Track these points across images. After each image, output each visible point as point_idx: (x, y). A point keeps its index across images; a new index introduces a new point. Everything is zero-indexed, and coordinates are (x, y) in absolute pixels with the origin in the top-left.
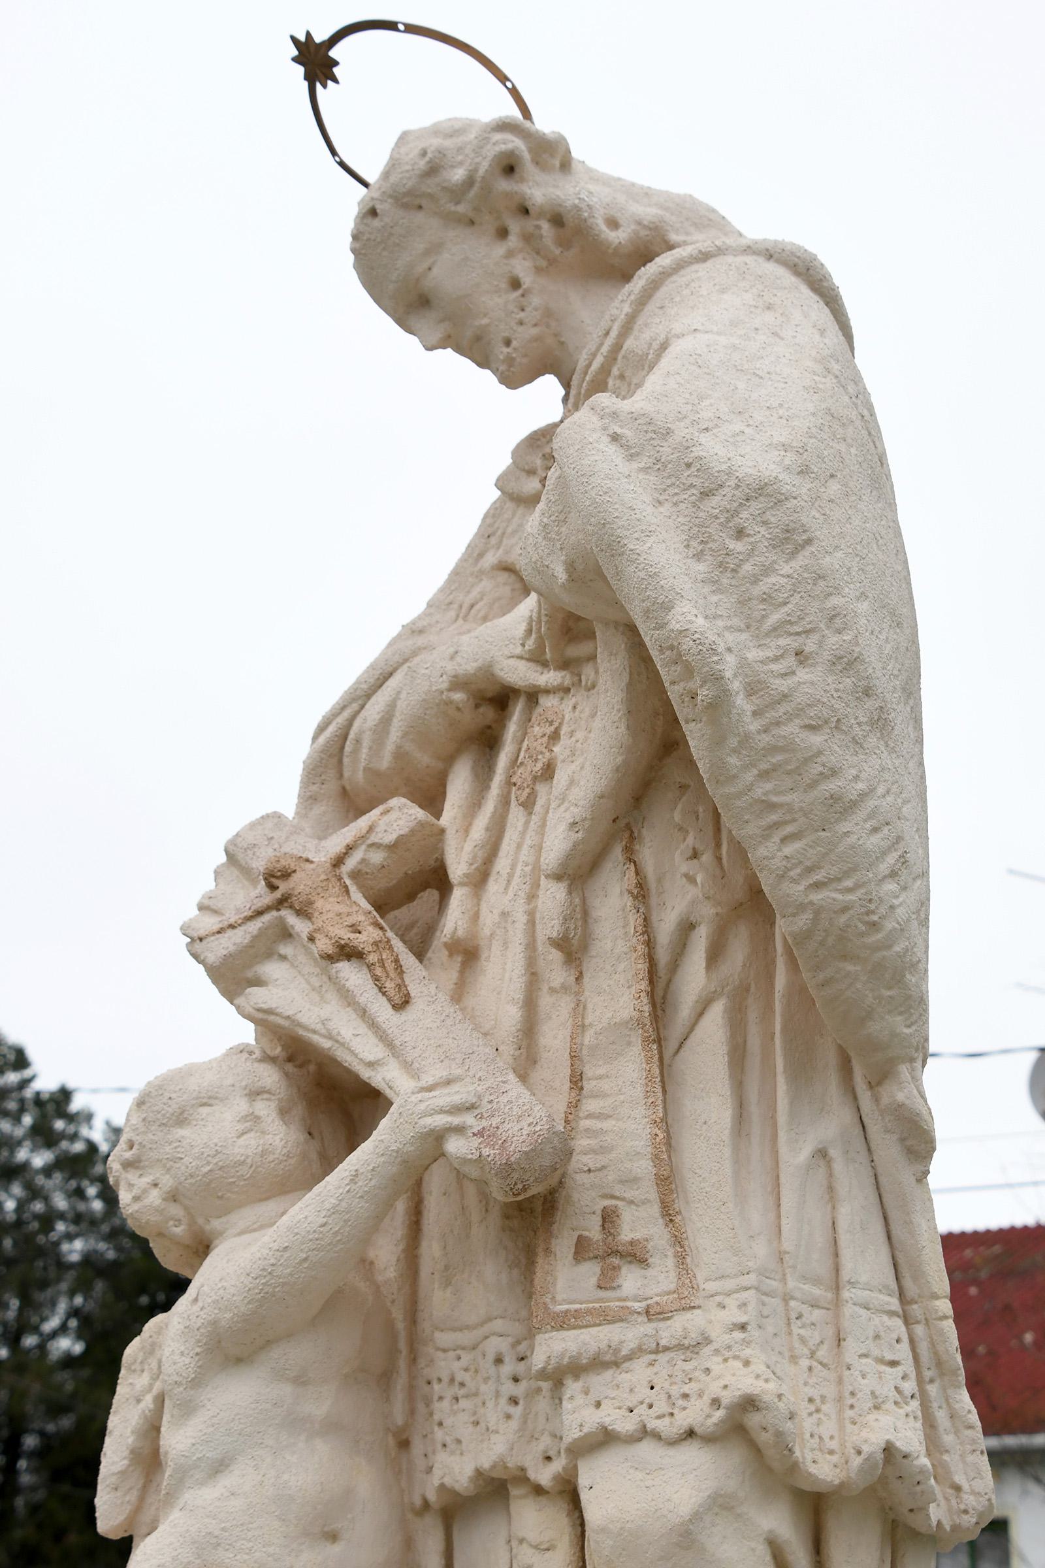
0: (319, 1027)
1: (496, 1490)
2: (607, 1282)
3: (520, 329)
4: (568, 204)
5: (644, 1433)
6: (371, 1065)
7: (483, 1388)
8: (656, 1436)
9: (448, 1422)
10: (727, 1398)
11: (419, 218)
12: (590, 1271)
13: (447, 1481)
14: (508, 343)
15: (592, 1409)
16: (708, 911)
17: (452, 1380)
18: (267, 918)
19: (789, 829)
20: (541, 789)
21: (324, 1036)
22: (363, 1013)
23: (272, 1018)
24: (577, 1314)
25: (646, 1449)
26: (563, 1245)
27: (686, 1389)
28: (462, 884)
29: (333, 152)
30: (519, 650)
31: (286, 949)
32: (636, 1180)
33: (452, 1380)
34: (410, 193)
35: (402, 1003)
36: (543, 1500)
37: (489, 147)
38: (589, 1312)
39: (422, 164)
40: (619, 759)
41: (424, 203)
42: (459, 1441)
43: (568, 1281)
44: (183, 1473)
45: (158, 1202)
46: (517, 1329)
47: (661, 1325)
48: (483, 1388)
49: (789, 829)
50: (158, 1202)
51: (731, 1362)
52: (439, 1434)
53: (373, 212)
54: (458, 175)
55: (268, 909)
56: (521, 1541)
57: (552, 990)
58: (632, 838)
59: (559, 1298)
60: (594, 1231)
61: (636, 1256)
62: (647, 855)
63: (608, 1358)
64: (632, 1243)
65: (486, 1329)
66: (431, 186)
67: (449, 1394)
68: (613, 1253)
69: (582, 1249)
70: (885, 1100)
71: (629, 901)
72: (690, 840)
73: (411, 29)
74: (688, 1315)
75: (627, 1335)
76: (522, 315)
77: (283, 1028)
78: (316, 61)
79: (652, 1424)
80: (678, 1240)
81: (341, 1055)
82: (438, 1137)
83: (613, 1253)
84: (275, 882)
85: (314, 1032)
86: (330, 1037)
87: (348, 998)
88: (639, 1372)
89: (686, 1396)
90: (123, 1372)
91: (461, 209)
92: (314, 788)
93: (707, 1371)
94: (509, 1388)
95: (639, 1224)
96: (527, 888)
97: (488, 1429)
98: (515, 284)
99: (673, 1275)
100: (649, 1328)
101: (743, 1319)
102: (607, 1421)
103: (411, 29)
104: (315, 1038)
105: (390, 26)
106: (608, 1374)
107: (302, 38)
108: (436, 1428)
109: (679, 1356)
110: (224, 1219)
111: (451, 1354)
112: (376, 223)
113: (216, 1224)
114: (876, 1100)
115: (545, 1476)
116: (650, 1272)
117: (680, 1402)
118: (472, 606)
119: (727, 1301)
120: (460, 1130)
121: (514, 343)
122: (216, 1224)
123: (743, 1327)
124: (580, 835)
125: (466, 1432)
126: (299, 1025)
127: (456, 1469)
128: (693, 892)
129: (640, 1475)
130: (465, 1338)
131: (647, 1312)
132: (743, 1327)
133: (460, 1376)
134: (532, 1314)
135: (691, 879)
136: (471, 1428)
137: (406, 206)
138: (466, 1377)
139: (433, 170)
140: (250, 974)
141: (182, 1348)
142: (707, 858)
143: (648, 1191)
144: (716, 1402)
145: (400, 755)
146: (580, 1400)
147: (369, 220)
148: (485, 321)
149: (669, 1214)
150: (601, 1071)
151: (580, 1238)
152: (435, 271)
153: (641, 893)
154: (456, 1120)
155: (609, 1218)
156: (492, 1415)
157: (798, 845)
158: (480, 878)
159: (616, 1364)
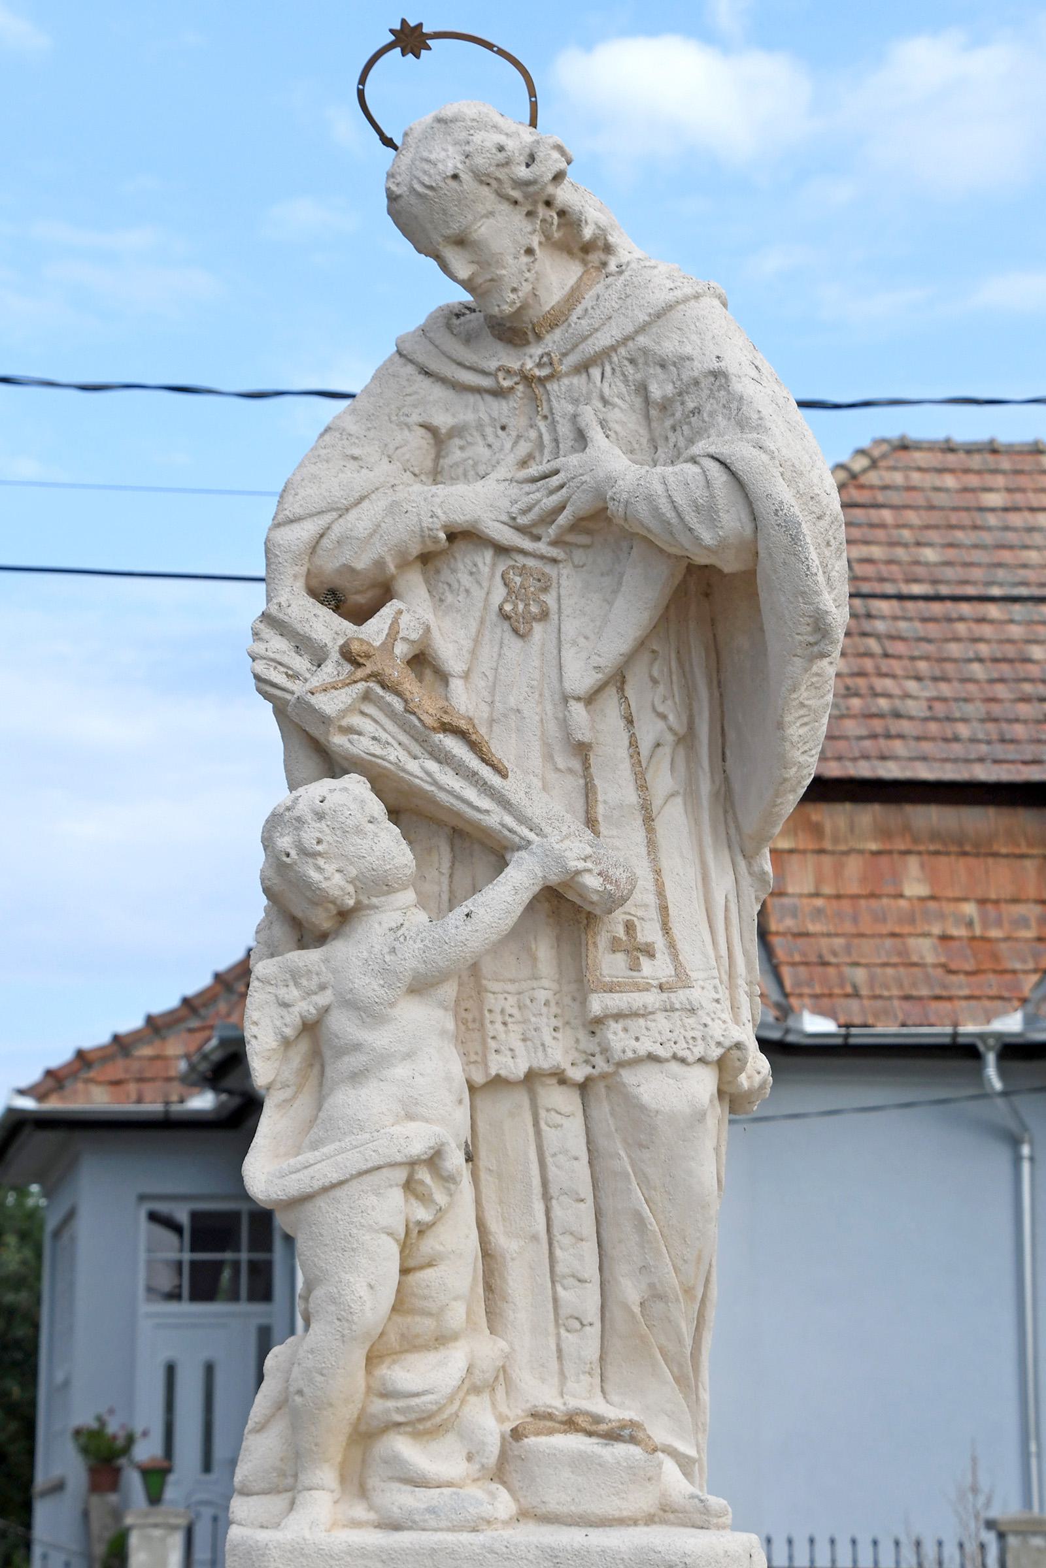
0: (422, 775)
1: (531, 1078)
2: (635, 967)
3: (524, 284)
4: (577, 208)
5: (675, 1057)
6: (487, 812)
7: (533, 1019)
8: (683, 1061)
9: (502, 1036)
10: (727, 1043)
11: (485, 191)
12: (620, 957)
13: (503, 1073)
14: (514, 290)
15: (633, 1042)
16: (669, 738)
17: (502, 1011)
18: (361, 686)
19: (806, 719)
20: (538, 628)
21: (427, 782)
22: (472, 777)
23: (380, 761)
24: (619, 984)
25: (674, 1066)
26: (603, 940)
27: (692, 1034)
28: (461, 677)
29: (363, 80)
30: (505, 518)
31: (370, 709)
32: (646, 906)
33: (502, 1011)
34: (488, 175)
35: (502, 773)
36: (563, 1088)
37: (550, 162)
38: (626, 984)
39: (501, 156)
40: (638, 633)
41: (494, 183)
42: (511, 1050)
43: (611, 965)
44: (383, 1060)
45: (343, 883)
46: (555, 986)
47: (671, 995)
48: (533, 1019)
49: (806, 719)
50: (343, 883)
51: (717, 1021)
52: (492, 1044)
53: (455, 177)
54: (522, 172)
55: (362, 680)
56: (548, 1110)
57: (557, 770)
58: (623, 682)
59: (605, 972)
60: (621, 932)
61: (649, 951)
62: (629, 692)
63: (642, 1012)
64: (648, 944)
65: (535, 984)
66: (501, 174)
67: (499, 1019)
68: (640, 951)
69: (615, 946)
70: (756, 869)
71: (622, 724)
72: (661, 689)
73: (502, 53)
74: (687, 991)
75: (652, 999)
76: (527, 275)
77: (385, 768)
78: (411, 40)
79: (680, 1054)
80: (672, 945)
81: (442, 796)
82: (578, 873)
83: (640, 951)
84: (361, 661)
85: (418, 777)
86: (435, 783)
87: (444, 758)
88: (661, 1022)
89: (693, 1038)
90: (254, 984)
91: (516, 194)
92: (297, 568)
93: (705, 1025)
94: (554, 1022)
95: (650, 933)
96: (536, 696)
97: (543, 1045)
98: (529, 251)
99: (672, 968)
100: (665, 996)
101: (717, 996)
102: (651, 1049)
103: (502, 53)
104: (417, 781)
105: (489, 46)
106: (641, 1021)
107: (412, 24)
108: (490, 1040)
109: (684, 1014)
110: (383, 899)
111: (501, 997)
112: (453, 184)
113: (374, 900)
114: (749, 865)
115: (578, 1074)
116: (655, 962)
117: (691, 1041)
118: (397, 448)
119: (707, 985)
120: (589, 871)
121: (520, 294)
122: (374, 900)
123: (717, 1001)
124: (600, 676)
125: (519, 1046)
126: (404, 770)
127: (517, 1068)
128: (661, 725)
129: (671, 1081)
130: (511, 987)
131: (661, 987)
132: (717, 1001)
133: (509, 1010)
134: (580, 981)
135: (664, 717)
136: (520, 1044)
137: (481, 182)
138: (515, 1011)
139: (507, 163)
140: (344, 723)
141: (382, 982)
142: (669, 702)
143: (654, 914)
144: (719, 1044)
145: (380, 564)
146: (621, 1034)
147: (450, 182)
148: (504, 272)
149: (666, 929)
150: (615, 833)
151: (614, 937)
152: (483, 229)
153: (630, 721)
154: (589, 865)
155: (629, 927)
156: (547, 1035)
157: (806, 729)
158: (466, 676)
159: (643, 1015)
